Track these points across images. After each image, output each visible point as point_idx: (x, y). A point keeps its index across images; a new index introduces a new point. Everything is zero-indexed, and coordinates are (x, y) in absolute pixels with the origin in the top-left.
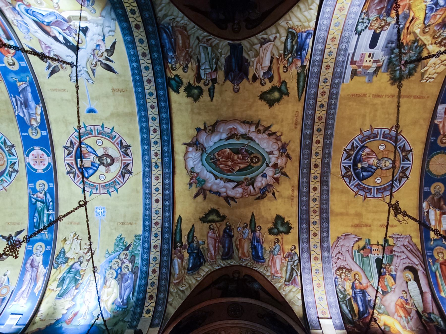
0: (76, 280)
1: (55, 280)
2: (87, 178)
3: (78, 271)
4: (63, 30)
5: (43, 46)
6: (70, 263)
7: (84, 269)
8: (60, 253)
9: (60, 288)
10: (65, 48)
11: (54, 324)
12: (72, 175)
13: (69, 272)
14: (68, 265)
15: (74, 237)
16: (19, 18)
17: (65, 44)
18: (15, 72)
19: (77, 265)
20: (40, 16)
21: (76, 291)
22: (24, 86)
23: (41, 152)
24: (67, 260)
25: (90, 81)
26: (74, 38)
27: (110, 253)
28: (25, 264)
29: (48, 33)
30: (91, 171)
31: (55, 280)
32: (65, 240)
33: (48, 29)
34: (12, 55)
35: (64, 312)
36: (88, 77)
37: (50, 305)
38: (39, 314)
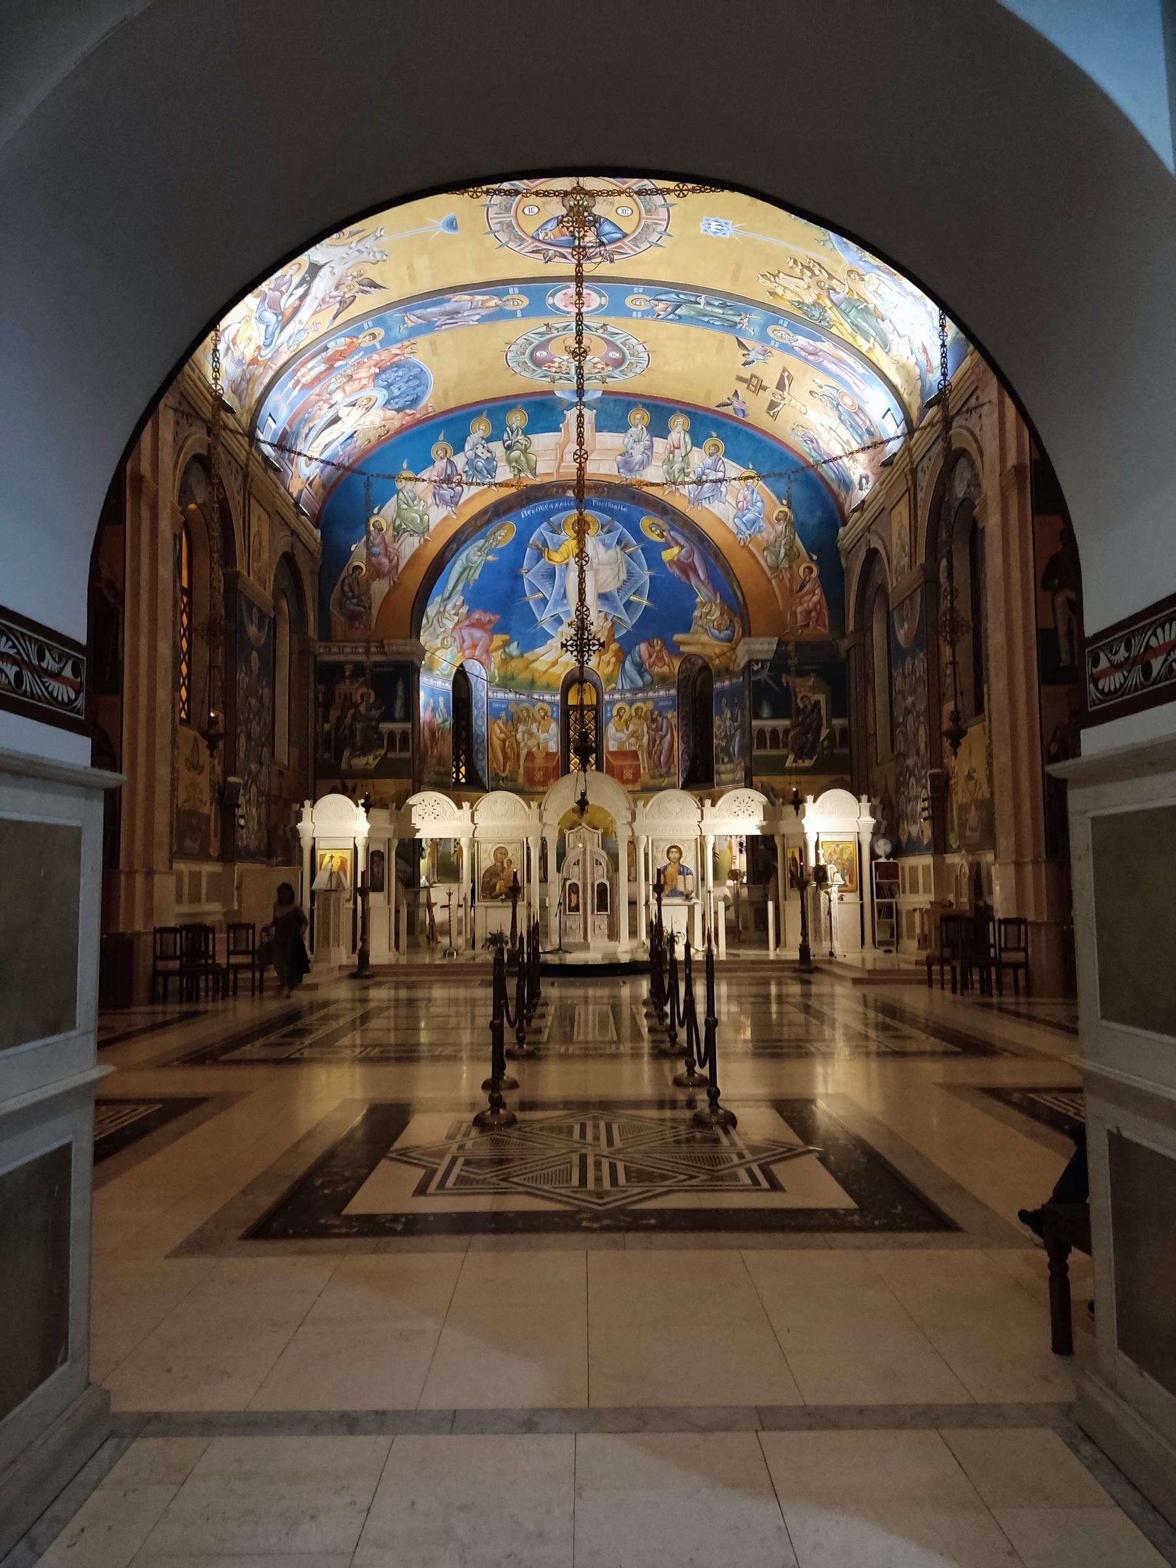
0: (866, 310)
1: (854, 338)
2: (625, 235)
3: (848, 300)
4: (282, 294)
5: (324, 307)
6: (829, 304)
7: (847, 290)
8: (800, 308)
9: (872, 340)
10: (317, 281)
11: (923, 386)
12: (616, 257)
13: (845, 313)
14: (830, 308)
15: (770, 280)
16: (285, 346)
17: (310, 283)
18: (388, 330)
19: (834, 297)
20: (271, 329)
21: (887, 321)
22: (413, 318)
23: (560, 295)
24: (815, 304)
25: (378, 234)
26: (291, 276)
27: (823, 238)
28: (806, 359)
29: (296, 310)
30: (607, 228)
31: (854, 338)
32: (773, 294)
33: (288, 312)
34: (355, 340)
35: (912, 360)
36: (372, 238)
37: (893, 367)
38: (901, 391)
